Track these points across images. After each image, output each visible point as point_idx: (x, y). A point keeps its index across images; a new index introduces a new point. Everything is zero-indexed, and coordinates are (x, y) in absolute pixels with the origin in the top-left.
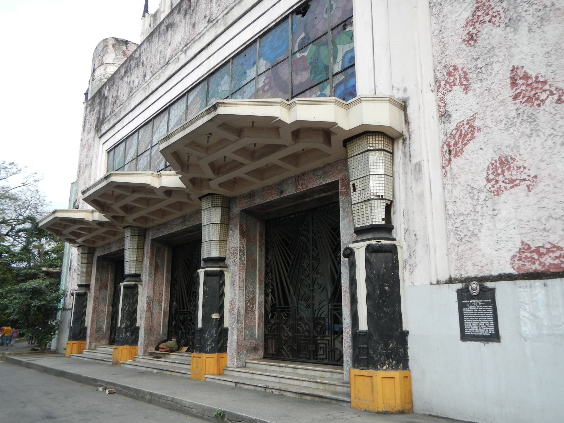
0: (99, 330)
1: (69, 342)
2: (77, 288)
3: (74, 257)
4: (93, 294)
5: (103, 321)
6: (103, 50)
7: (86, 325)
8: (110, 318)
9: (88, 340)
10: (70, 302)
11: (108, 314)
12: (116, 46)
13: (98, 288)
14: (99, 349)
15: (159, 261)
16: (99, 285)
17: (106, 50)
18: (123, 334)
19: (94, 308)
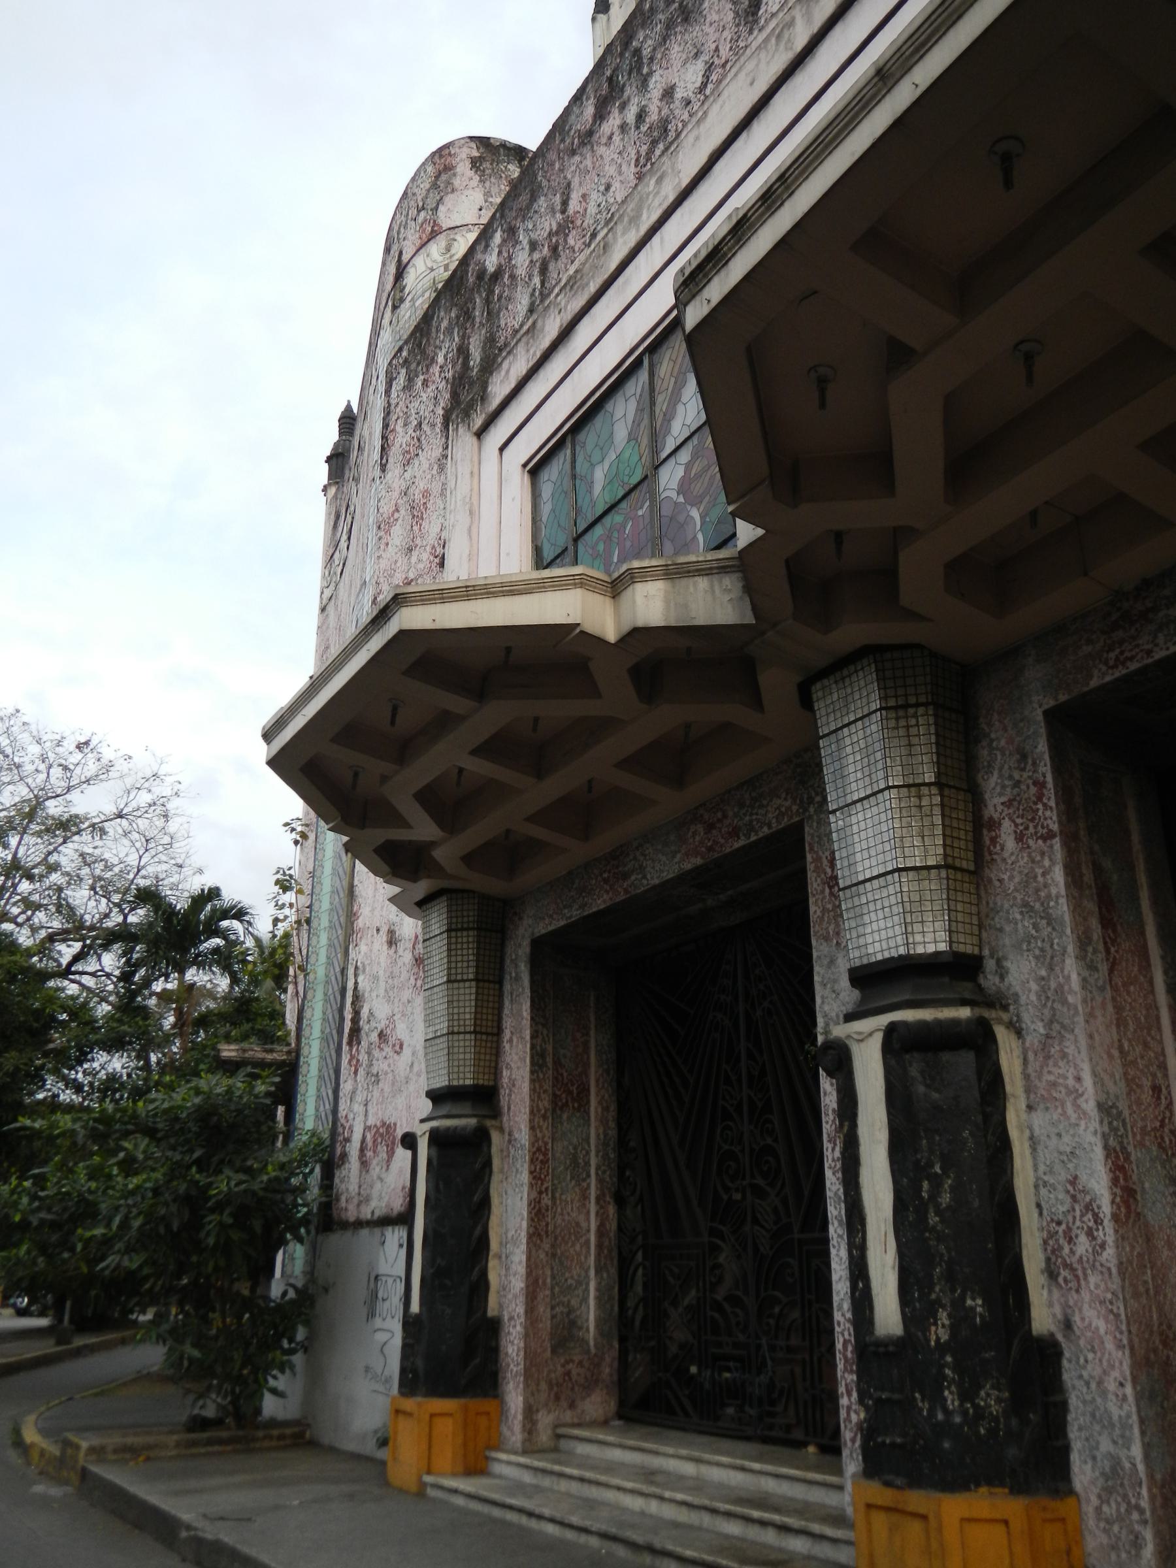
0: (565, 1334)
1: (409, 1404)
2: (426, 1106)
3: (376, 978)
4: (523, 1136)
5: (582, 1282)
6: (435, 186)
7: (492, 1310)
8: (613, 1271)
9: (515, 1398)
10: (388, 1181)
11: (599, 1246)
12: (487, 165)
13: (545, 1103)
14: (582, 1449)
15: (1107, 864)
16: (547, 1086)
17: (448, 183)
18: (951, 1399)
19: (537, 1213)
